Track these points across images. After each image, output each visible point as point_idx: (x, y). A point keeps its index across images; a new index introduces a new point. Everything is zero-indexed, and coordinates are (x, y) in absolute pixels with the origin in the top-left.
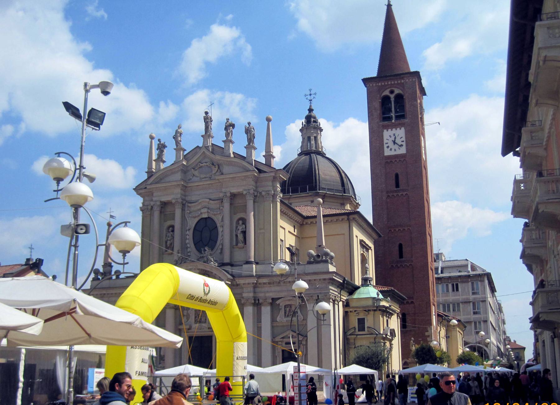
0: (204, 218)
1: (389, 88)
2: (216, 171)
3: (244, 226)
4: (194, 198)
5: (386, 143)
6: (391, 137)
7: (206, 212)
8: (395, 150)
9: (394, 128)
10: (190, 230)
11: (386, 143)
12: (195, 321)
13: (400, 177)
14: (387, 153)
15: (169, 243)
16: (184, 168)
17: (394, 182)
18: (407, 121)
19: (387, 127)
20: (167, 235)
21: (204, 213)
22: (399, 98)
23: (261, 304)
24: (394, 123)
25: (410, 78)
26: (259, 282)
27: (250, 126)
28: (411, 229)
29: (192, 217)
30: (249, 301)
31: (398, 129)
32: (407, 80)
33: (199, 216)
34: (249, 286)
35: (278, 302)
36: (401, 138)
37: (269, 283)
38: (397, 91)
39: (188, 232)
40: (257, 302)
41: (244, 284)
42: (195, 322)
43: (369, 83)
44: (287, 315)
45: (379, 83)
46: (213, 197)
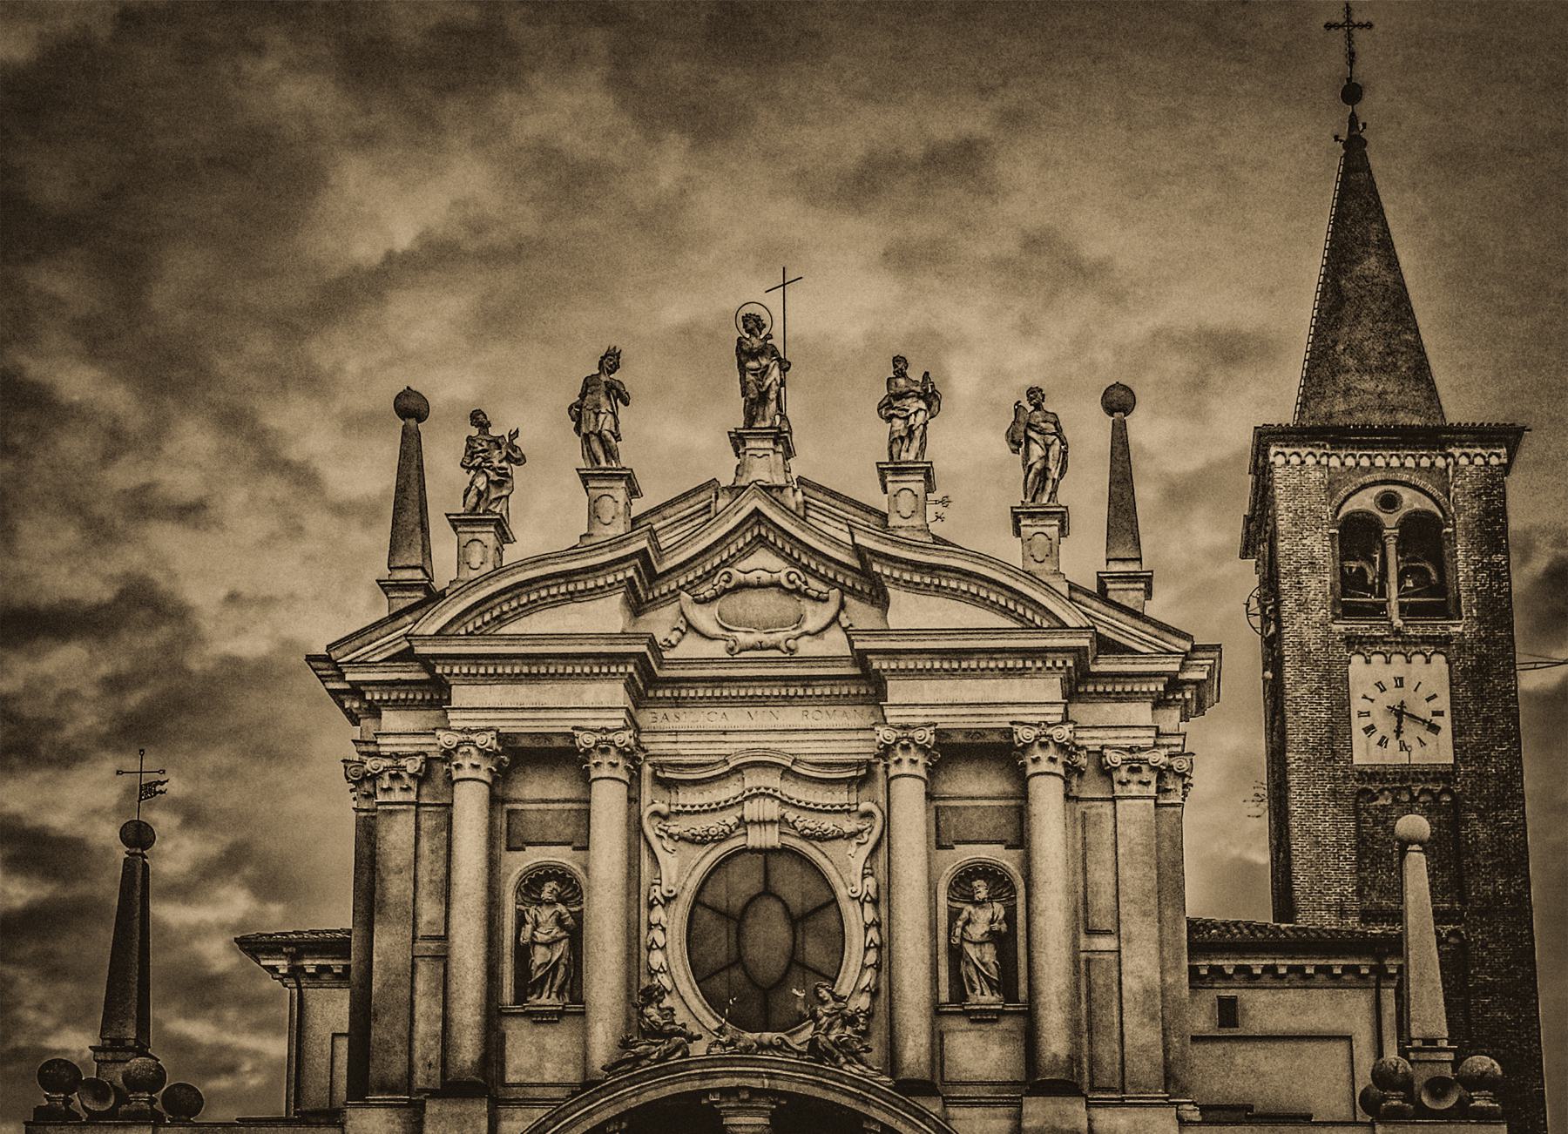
0: (754, 850)
2: (827, 620)
4: (689, 750)
7: (772, 822)
16: (641, 579)
21: (762, 823)
27: (1038, 407)
33: (726, 837)
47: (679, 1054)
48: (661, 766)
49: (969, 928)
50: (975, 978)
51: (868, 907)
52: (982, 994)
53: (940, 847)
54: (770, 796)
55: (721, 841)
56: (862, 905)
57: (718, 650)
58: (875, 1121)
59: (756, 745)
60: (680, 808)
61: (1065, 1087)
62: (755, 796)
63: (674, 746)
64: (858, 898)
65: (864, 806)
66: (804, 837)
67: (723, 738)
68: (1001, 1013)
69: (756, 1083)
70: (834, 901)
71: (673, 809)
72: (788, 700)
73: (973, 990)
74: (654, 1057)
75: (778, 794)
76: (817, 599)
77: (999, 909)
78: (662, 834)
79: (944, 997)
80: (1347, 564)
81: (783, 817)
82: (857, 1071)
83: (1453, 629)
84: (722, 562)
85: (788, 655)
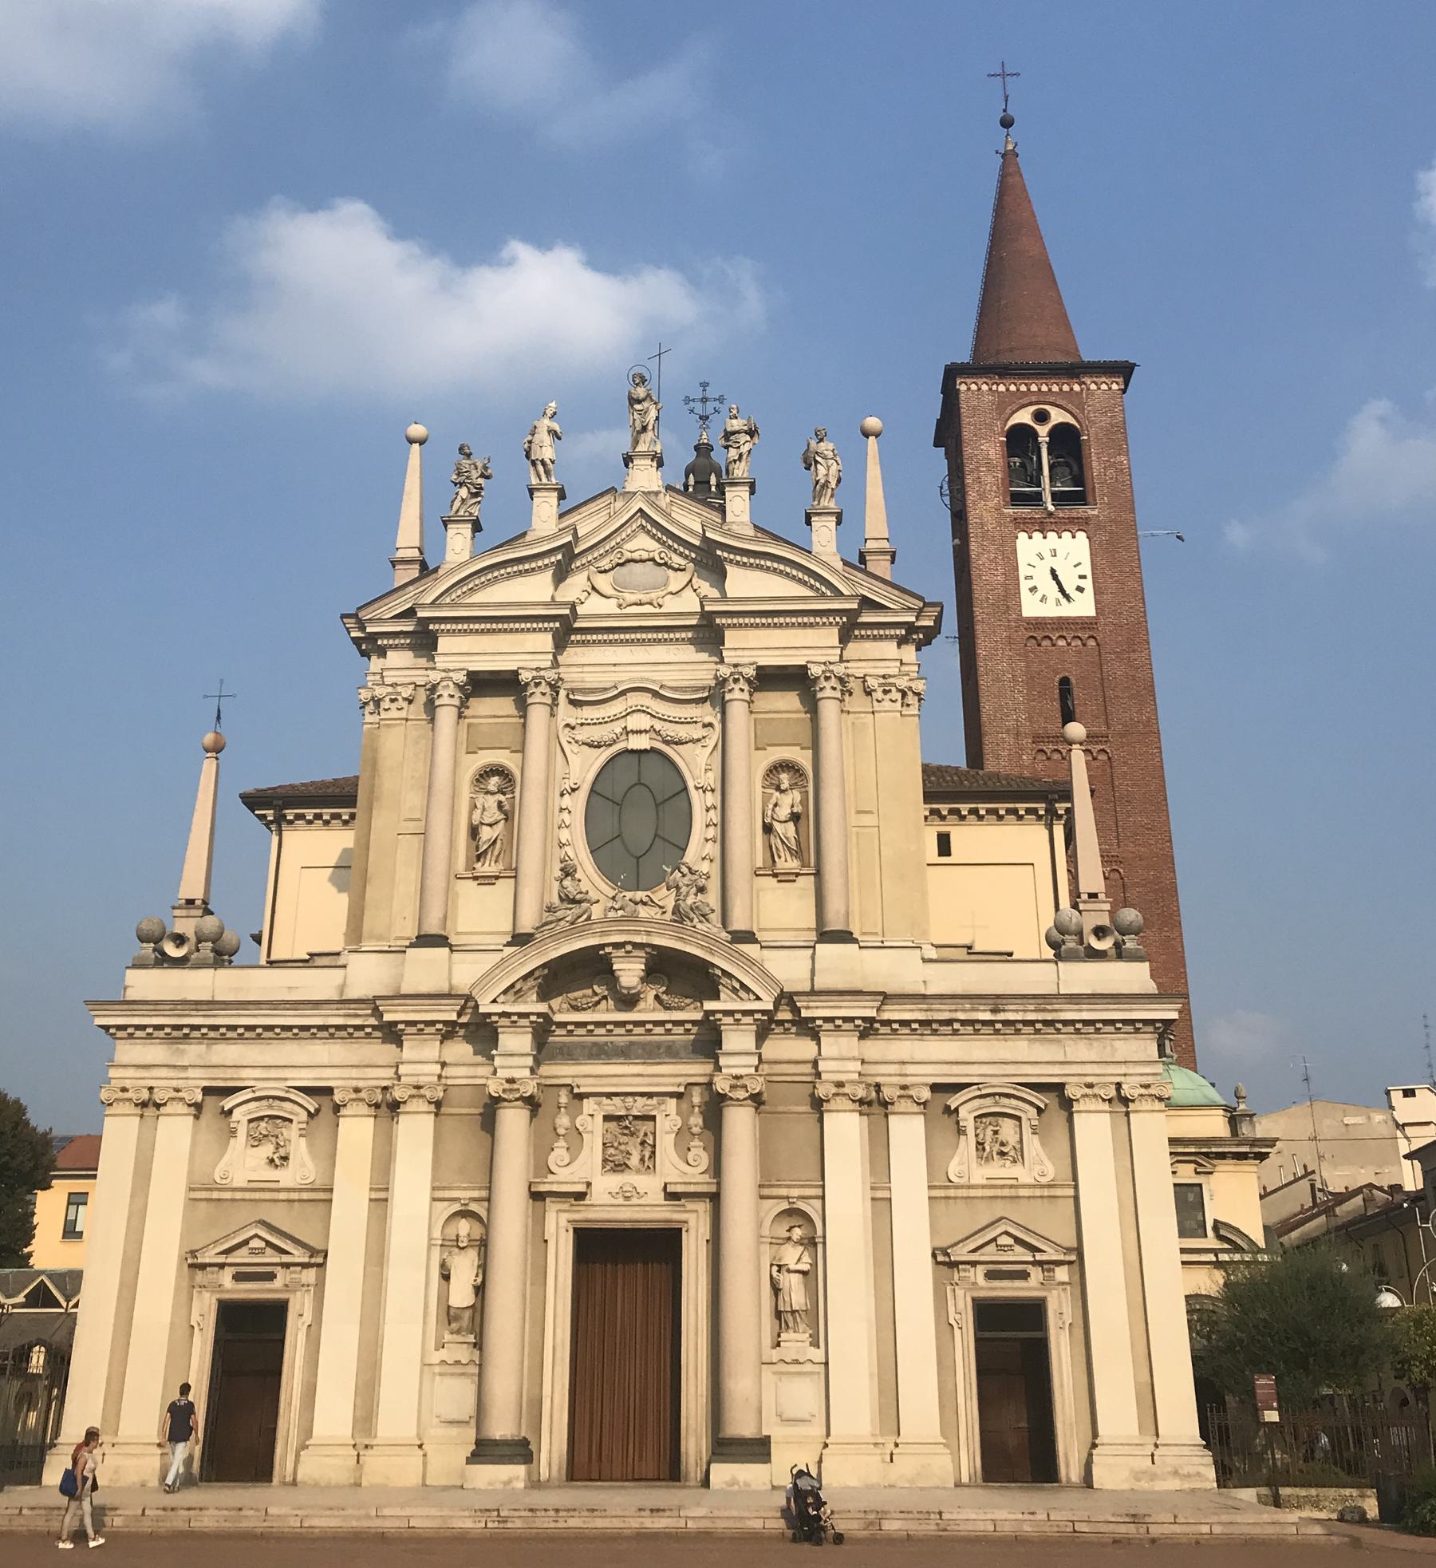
0: (633, 751)
1: (1031, 404)
3: (796, 795)
4: (592, 679)
7: (646, 731)
12: (605, 1161)
15: (486, 834)
23: (885, 1104)
25: (1104, 379)
26: (886, 1016)
30: (847, 1090)
32: (1093, 387)
34: (846, 1026)
38: (1057, 416)
39: (567, 801)
40: (874, 1094)
41: (826, 1020)
42: (604, 1167)
44: (985, 1154)
46: (671, 677)
48: (573, 691)
50: (781, 850)
51: (709, 794)
52: (786, 861)
53: (757, 749)
54: (644, 711)
55: (610, 745)
56: (704, 792)
57: (610, 606)
58: (718, 967)
60: (583, 721)
61: (844, 937)
62: (634, 711)
63: (581, 675)
64: (702, 787)
65: (707, 720)
66: (667, 743)
67: (613, 669)
68: (797, 875)
70: (685, 789)
71: (579, 721)
73: (780, 857)
75: (649, 710)
76: (676, 570)
77: (796, 795)
78: (571, 740)
79: (760, 864)
80: (1012, 459)
81: (652, 727)
82: (706, 929)
85: (657, 610)
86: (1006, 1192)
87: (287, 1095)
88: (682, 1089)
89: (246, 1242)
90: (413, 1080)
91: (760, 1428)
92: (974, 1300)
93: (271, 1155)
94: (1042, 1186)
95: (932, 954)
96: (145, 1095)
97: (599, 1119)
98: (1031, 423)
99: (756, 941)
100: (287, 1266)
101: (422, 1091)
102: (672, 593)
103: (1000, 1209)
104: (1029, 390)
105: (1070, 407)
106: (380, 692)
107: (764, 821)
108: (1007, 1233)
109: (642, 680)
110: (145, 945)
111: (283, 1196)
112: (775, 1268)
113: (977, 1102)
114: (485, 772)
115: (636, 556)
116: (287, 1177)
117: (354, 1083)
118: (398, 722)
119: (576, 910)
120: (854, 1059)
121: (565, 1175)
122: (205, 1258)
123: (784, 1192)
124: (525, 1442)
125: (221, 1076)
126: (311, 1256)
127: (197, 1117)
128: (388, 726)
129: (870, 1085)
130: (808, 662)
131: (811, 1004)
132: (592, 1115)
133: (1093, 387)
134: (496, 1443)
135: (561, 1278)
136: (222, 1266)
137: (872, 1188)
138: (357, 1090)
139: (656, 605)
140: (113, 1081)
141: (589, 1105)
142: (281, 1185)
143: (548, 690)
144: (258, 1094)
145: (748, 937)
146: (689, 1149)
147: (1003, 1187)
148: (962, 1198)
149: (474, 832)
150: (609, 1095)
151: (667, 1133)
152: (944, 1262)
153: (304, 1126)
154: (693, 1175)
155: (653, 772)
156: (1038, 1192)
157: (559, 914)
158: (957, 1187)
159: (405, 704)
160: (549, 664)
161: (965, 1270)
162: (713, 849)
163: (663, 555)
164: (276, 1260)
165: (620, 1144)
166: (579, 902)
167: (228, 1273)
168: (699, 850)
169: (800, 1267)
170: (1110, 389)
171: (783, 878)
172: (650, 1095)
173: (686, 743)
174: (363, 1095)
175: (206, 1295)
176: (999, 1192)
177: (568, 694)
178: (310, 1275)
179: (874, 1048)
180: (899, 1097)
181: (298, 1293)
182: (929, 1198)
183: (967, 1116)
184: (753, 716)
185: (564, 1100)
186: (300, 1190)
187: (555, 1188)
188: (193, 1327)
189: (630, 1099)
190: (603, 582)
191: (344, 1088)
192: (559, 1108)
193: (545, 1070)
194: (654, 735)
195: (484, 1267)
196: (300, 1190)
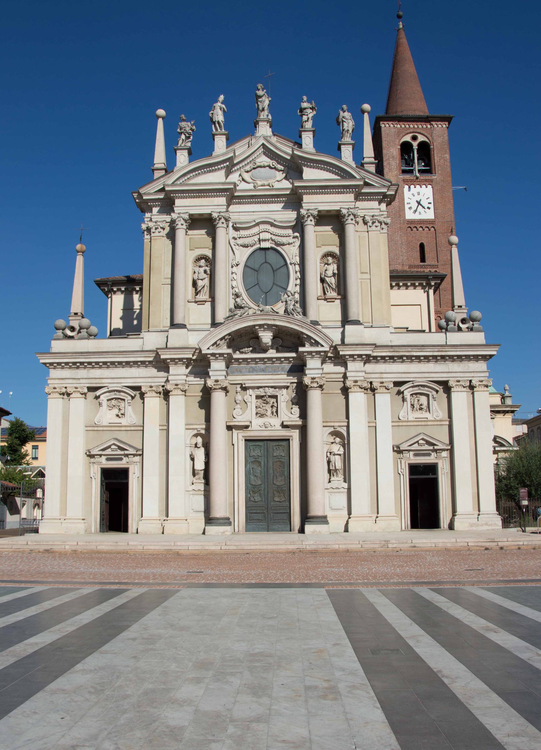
1: (410, 133)
4: (243, 218)
5: (408, 203)
6: (414, 196)
7: (268, 240)
8: (420, 213)
9: (418, 185)
10: (239, 266)
11: (408, 203)
12: (257, 414)
13: (426, 249)
14: (409, 215)
15: (200, 283)
17: (418, 254)
18: (436, 177)
19: (409, 183)
20: (196, 271)
21: (265, 240)
22: (425, 148)
24: (417, 178)
25: (440, 123)
28: (441, 317)
29: (241, 246)
31: (424, 186)
32: (436, 126)
35: (402, 389)
36: (427, 199)
37: (391, 358)
38: (421, 138)
43: (385, 123)
44: (414, 409)
45: (397, 124)
47: (246, 313)
49: (327, 272)
52: (331, 293)
53: (318, 247)
54: (267, 232)
55: (252, 246)
56: (295, 265)
57: (251, 186)
59: (263, 216)
60: (240, 236)
61: (357, 322)
67: (253, 214)
69: (270, 322)
70: (286, 264)
71: (239, 236)
72: (272, 202)
73: (328, 292)
74: (239, 315)
75: (270, 231)
81: (271, 238)
83: (434, 177)
84: (253, 160)
86: (423, 423)
87: (122, 389)
88: (289, 384)
89: (109, 447)
90: (176, 382)
91: (324, 512)
92: (409, 464)
93: (117, 413)
94: (438, 421)
95: (393, 331)
96: (64, 390)
97: (254, 397)
98: (410, 141)
99: (319, 325)
100: (127, 455)
101: (179, 386)
102: (278, 181)
103: (420, 430)
104: (410, 127)
105: (426, 134)
106: (151, 224)
107: (321, 277)
108: (423, 439)
109: (266, 218)
110: (58, 331)
111: (123, 429)
112: (328, 454)
113: (411, 389)
114: (198, 258)
115: (262, 164)
116: (124, 421)
117: (150, 384)
118: (159, 237)
119: (242, 311)
120: (362, 371)
121: (240, 419)
122: (93, 453)
123: (332, 424)
124: (228, 519)
125: (94, 382)
126: (137, 452)
127: (86, 398)
128: (155, 239)
129: (368, 382)
130: (340, 208)
131: (344, 349)
132: (251, 395)
133: (436, 126)
134: (218, 519)
135: (240, 458)
136: (101, 455)
137: (369, 422)
138: (151, 387)
139: (271, 186)
140: (50, 385)
141: (250, 392)
142: (123, 424)
143: (224, 221)
144: (110, 389)
145: (315, 323)
146: (292, 408)
147: (421, 421)
148: (405, 426)
149: (195, 284)
150: (258, 388)
151: (283, 402)
152: (398, 450)
153: (130, 401)
154: (294, 418)
155: (272, 257)
156: (436, 423)
157: (235, 313)
158: (403, 422)
159: (162, 230)
160: (225, 210)
161: (405, 453)
162: (298, 289)
163: (274, 164)
164: (122, 453)
165: (263, 406)
166: (242, 308)
167: (104, 458)
168: (293, 286)
169: (339, 453)
170: (442, 127)
171: (330, 300)
172: (275, 387)
173: (286, 245)
174: (154, 388)
175: (96, 466)
176: (420, 423)
177: (233, 225)
178: (137, 459)
179: (370, 367)
180: (380, 386)
181: (133, 465)
182: (392, 426)
183: (407, 394)
184: (315, 233)
185: (239, 389)
186: (130, 426)
187: (237, 424)
188: (91, 478)
189: (267, 389)
190: (246, 176)
191: (146, 386)
192: (237, 393)
193: (229, 378)
194: (270, 241)
195: (207, 455)
196: (130, 426)
